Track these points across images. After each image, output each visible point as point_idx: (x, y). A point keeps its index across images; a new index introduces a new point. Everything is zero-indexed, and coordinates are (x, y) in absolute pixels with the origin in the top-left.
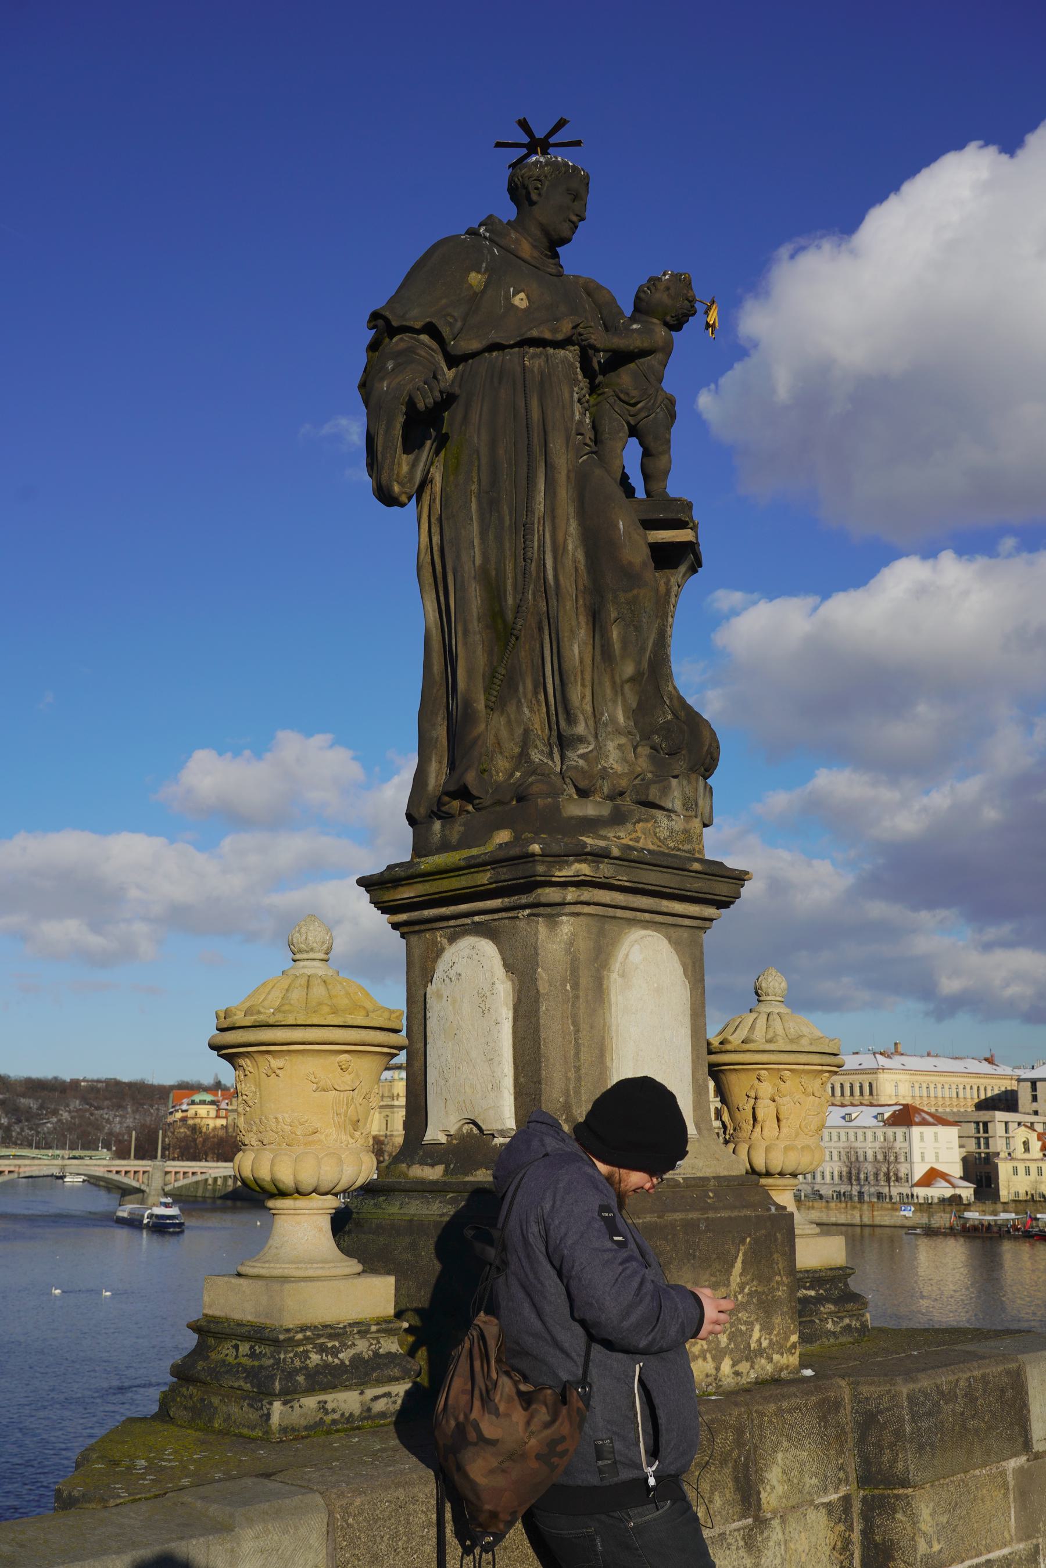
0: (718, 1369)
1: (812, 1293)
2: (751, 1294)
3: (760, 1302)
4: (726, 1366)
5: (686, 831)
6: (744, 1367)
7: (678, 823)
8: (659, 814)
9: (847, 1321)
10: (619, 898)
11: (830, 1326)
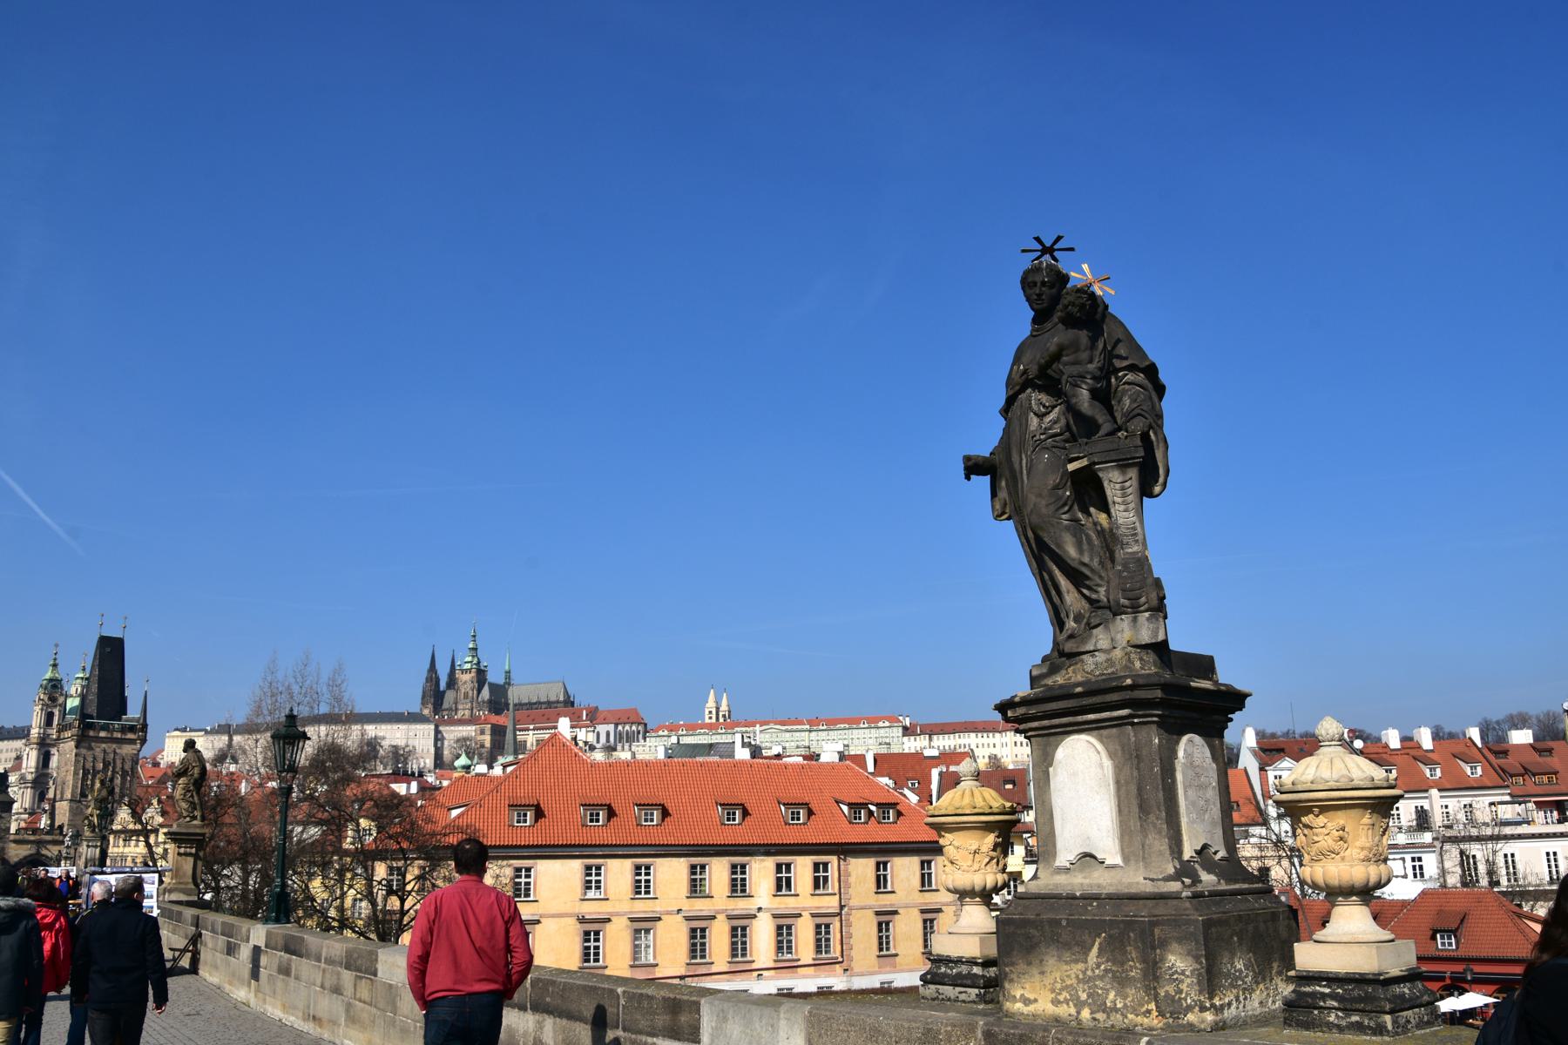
0: (1078, 1013)
1: (1327, 991)
2: (1106, 971)
3: (1114, 977)
4: (1086, 1014)
5: (1107, 660)
6: (1100, 1016)
7: (1100, 657)
8: (1084, 657)
9: (1355, 1018)
10: (1046, 723)
11: (1332, 1018)
